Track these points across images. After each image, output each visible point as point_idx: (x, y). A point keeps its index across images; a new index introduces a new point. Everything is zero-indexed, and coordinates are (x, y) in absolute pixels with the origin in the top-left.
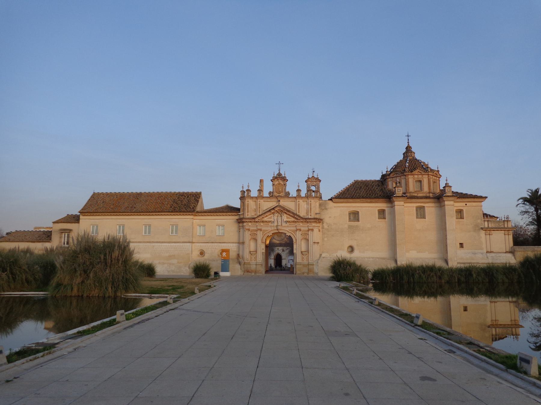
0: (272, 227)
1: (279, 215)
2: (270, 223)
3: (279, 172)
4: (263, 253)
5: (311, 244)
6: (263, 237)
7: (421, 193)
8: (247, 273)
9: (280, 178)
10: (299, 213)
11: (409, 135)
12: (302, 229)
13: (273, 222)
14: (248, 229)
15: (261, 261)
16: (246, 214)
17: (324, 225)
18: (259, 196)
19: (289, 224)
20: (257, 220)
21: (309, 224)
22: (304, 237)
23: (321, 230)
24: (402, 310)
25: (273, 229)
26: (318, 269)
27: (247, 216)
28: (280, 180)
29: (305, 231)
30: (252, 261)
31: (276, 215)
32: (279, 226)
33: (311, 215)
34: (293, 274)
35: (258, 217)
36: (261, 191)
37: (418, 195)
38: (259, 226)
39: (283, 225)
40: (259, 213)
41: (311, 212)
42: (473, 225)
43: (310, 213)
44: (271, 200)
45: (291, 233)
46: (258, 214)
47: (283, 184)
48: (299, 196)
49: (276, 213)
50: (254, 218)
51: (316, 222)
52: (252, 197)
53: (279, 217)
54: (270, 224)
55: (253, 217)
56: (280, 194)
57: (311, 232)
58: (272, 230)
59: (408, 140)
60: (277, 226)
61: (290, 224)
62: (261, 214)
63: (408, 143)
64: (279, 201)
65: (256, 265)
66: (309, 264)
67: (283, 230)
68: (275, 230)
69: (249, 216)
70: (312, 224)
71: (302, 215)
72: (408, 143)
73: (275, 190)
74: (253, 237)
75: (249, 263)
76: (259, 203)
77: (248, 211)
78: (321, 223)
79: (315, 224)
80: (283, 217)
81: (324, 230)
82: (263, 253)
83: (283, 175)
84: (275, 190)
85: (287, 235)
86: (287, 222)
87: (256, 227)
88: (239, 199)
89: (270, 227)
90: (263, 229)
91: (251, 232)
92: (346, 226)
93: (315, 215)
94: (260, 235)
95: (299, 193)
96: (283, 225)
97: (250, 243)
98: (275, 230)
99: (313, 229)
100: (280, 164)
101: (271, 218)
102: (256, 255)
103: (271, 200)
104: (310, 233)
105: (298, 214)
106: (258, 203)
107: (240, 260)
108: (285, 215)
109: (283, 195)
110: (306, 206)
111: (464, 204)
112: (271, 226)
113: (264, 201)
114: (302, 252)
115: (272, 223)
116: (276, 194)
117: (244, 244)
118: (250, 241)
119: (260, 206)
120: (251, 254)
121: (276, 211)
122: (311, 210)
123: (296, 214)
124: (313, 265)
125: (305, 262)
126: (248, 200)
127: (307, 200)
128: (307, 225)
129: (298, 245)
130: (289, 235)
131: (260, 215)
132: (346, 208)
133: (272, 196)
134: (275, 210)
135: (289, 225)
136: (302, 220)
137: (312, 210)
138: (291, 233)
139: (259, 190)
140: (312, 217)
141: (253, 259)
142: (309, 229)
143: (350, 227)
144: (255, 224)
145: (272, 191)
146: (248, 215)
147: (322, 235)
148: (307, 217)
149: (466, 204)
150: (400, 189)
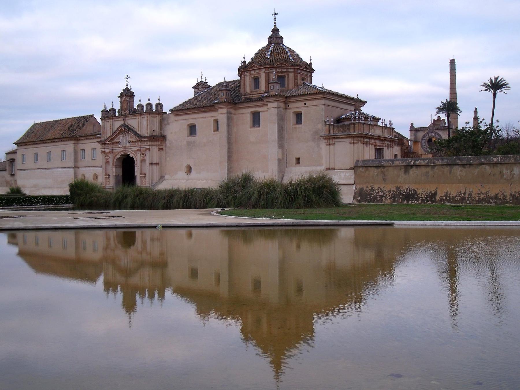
7: (256, 94)
10: (138, 131)
11: (273, 13)
24: (138, 240)
37: (254, 97)
42: (312, 133)
59: (275, 20)
63: (275, 23)
72: (275, 23)
92: (185, 143)
94: (111, 156)
111: (302, 104)
132: (185, 121)
143: (189, 143)
149: (305, 104)
150: (271, 86)
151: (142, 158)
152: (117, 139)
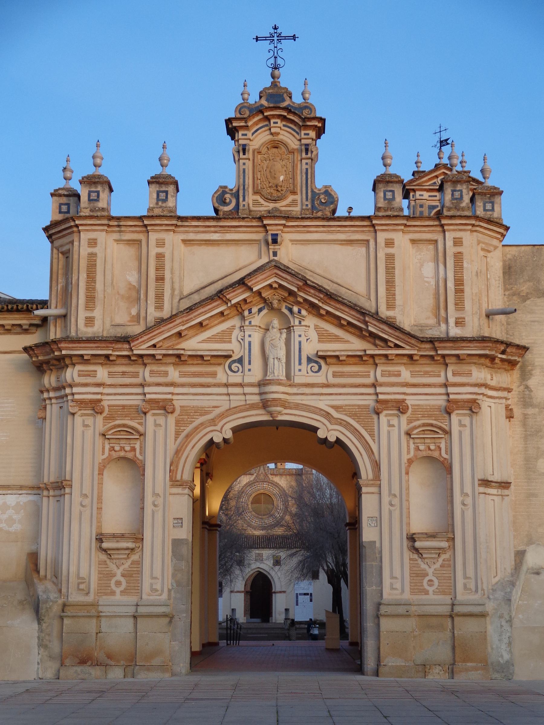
0: (231, 390)
1: (276, 323)
2: (219, 370)
3: (274, 85)
4: (176, 543)
5: (468, 489)
6: (178, 452)
8: (79, 669)
9: (279, 108)
10: (391, 306)
12: (410, 401)
13: (240, 361)
14: (92, 401)
15: (165, 596)
16: (82, 314)
17: (532, 382)
18: (157, 212)
19: (335, 375)
20: (142, 349)
21: (454, 374)
22: (422, 447)
23: (517, 412)
25: (237, 401)
26: (510, 644)
27: (86, 325)
28: (280, 123)
29: (430, 416)
30: (113, 593)
31: (258, 320)
32: (279, 383)
33: (459, 323)
34: (360, 670)
35: (148, 330)
36: (166, 184)
38: (158, 385)
39: (298, 380)
40: (159, 307)
41: (459, 304)
43: (457, 309)
44: (229, 236)
45: (347, 426)
46: (153, 314)
47: (293, 144)
48: (392, 209)
49: (255, 310)
50: (126, 340)
51: (492, 359)
52: (118, 219)
53: (274, 333)
54: (222, 375)
55: (119, 332)
56: (281, 205)
57: (466, 421)
58: (230, 411)
60: (261, 384)
61: (342, 375)
62: (166, 313)
64: (275, 241)
65: (135, 617)
66: (457, 609)
67: (297, 406)
68: (253, 407)
69: (96, 330)
70: (470, 374)
71: (406, 323)
73: (249, 181)
74: (117, 448)
75: (94, 605)
76: (160, 250)
77: (91, 300)
78: (516, 373)
79: (489, 377)
80: (298, 331)
81: (530, 411)
82: (176, 543)
83: (297, 99)
84: (249, 181)
85: (321, 434)
86: (324, 358)
87: (139, 390)
88: (44, 235)
89: (224, 390)
90: (177, 404)
91: (105, 418)
93: (484, 320)
95: (389, 195)
96: (298, 380)
97: (101, 483)
98: (253, 407)
99: (474, 401)
100: (281, 38)
101: (224, 337)
102: (135, 557)
103: (229, 236)
104: (461, 425)
105: (384, 312)
106: (154, 251)
107: (40, 588)
108: (311, 321)
109: (298, 209)
110: (429, 269)
112: (226, 385)
113: (185, 242)
114: (412, 538)
115: (234, 367)
116: (256, 203)
117: (67, 490)
118: (101, 473)
119: (160, 268)
120: (105, 550)
121: (259, 293)
122: (462, 291)
123: (377, 313)
124: (483, 615)
125: (432, 597)
126: (92, 235)
127: (440, 237)
128: (441, 380)
129: (386, 499)
130: (332, 439)
131: (161, 322)
133: (235, 214)
134: (251, 289)
135: (332, 380)
136: (412, 346)
137: (467, 289)
138: (347, 426)
139: (155, 181)
140: (468, 332)
141: (118, 583)
142: (456, 402)
144: (135, 375)
145: (231, 184)
146: (90, 321)
147: (526, 438)
148: (439, 332)
151: (417, 449)
152: (203, 341)
